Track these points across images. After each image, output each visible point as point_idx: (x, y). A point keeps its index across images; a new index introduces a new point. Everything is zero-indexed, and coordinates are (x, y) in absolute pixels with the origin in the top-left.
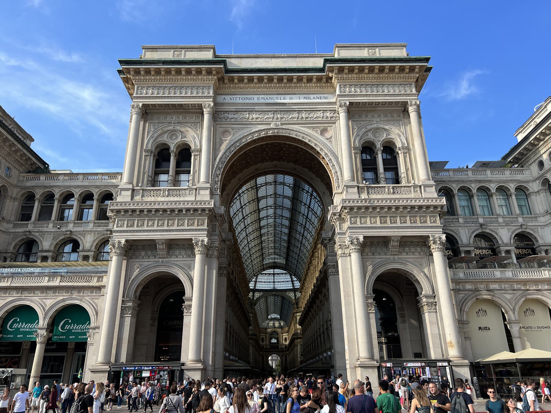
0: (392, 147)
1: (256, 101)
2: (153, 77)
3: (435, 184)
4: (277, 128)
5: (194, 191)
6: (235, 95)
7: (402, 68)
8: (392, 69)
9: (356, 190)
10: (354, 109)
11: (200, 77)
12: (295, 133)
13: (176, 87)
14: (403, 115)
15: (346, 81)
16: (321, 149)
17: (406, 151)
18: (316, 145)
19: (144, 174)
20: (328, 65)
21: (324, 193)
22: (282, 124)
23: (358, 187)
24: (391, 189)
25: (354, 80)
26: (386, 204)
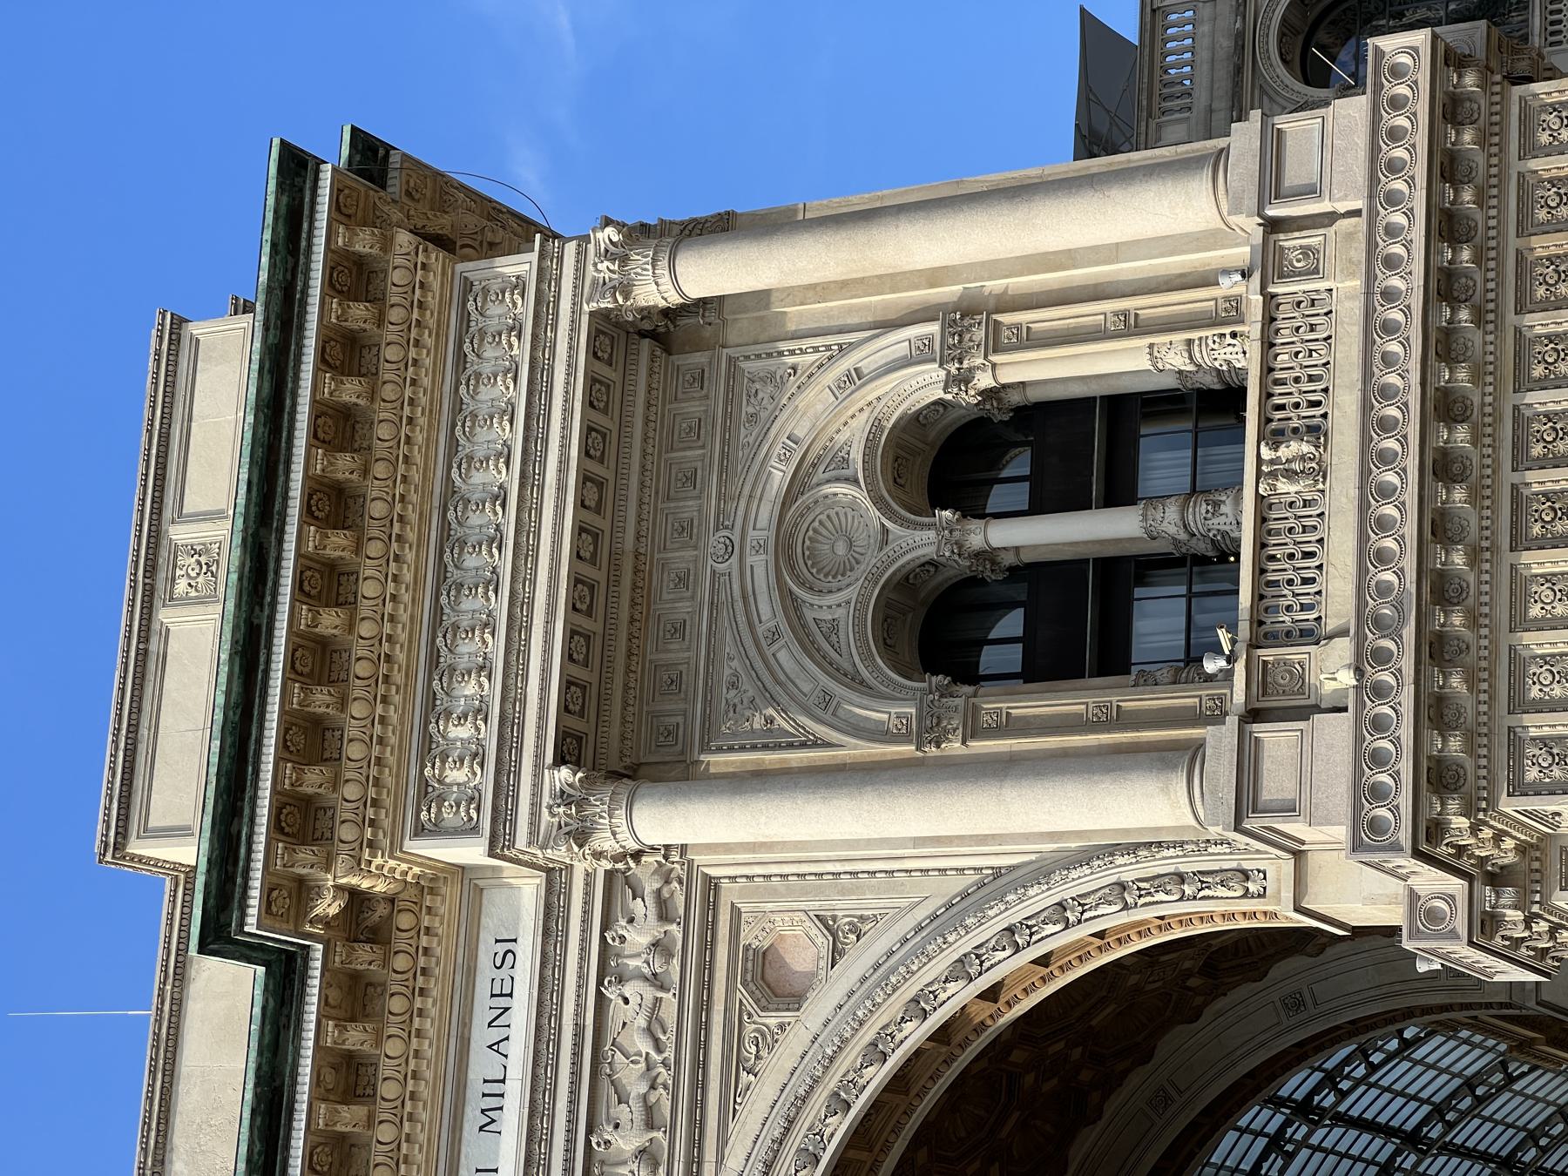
0: (937, 434)
3: (1256, 115)
7: (335, 351)
9: (1276, 738)
10: (615, 730)
14: (698, 347)
15: (389, 780)
16: (917, 1008)
17: (979, 334)
18: (876, 1053)
20: (251, 926)
21: (1295, 1003)
23: (1253, 715)
24: (1284, 452)
25: (394, 717)
26: (1411, 497)
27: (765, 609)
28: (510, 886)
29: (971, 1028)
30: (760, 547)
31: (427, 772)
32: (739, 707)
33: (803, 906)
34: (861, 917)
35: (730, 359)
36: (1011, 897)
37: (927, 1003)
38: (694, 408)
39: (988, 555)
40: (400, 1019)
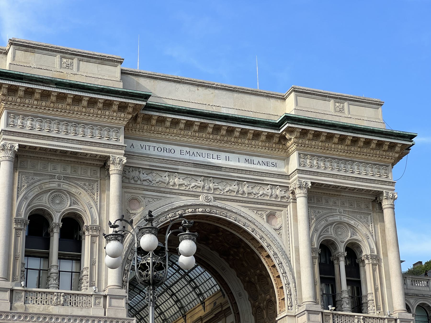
1: (177, 155)
2: (36, 102)
3: (413, 318)
4: (210, 206)
5: (102, 299)
6: (148, 141)
8: (368, 142)
9: (319, 317)
11: (107, 113)
12: (234, 216)
13: (69, 121)
14: (373, 207)
15: (308, 149)
18: (261, 238)
19: (16, 259)
21: (240, 295)
22: (215, 199)
23: (322, 313)
24: (361, 320)
27: (331, 219)
28: (285, 166)
29: (261, 251)
30: (341, 218)
31: (309, 156)
32: (315, 213)
33: (283, 223)
34: (281, 234)
35: (371, 214)
36: (287, 264)
37: (270, 247)
38: (363, 206)
39: (338, 259)
40: (265, 145)
